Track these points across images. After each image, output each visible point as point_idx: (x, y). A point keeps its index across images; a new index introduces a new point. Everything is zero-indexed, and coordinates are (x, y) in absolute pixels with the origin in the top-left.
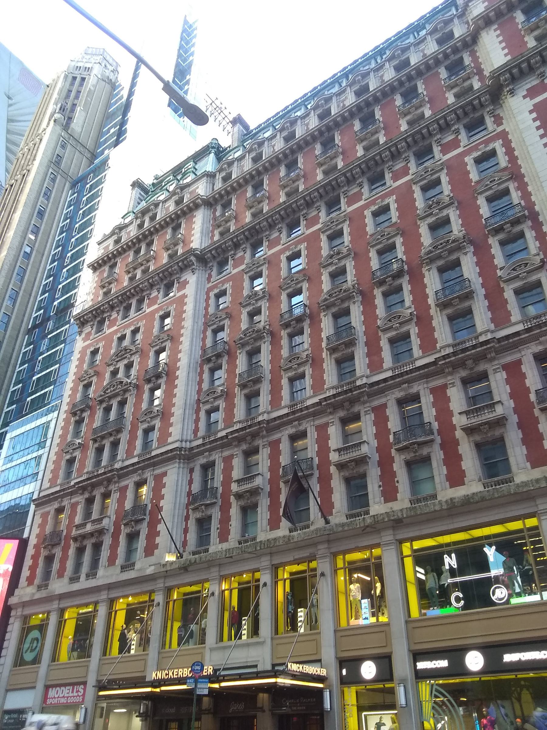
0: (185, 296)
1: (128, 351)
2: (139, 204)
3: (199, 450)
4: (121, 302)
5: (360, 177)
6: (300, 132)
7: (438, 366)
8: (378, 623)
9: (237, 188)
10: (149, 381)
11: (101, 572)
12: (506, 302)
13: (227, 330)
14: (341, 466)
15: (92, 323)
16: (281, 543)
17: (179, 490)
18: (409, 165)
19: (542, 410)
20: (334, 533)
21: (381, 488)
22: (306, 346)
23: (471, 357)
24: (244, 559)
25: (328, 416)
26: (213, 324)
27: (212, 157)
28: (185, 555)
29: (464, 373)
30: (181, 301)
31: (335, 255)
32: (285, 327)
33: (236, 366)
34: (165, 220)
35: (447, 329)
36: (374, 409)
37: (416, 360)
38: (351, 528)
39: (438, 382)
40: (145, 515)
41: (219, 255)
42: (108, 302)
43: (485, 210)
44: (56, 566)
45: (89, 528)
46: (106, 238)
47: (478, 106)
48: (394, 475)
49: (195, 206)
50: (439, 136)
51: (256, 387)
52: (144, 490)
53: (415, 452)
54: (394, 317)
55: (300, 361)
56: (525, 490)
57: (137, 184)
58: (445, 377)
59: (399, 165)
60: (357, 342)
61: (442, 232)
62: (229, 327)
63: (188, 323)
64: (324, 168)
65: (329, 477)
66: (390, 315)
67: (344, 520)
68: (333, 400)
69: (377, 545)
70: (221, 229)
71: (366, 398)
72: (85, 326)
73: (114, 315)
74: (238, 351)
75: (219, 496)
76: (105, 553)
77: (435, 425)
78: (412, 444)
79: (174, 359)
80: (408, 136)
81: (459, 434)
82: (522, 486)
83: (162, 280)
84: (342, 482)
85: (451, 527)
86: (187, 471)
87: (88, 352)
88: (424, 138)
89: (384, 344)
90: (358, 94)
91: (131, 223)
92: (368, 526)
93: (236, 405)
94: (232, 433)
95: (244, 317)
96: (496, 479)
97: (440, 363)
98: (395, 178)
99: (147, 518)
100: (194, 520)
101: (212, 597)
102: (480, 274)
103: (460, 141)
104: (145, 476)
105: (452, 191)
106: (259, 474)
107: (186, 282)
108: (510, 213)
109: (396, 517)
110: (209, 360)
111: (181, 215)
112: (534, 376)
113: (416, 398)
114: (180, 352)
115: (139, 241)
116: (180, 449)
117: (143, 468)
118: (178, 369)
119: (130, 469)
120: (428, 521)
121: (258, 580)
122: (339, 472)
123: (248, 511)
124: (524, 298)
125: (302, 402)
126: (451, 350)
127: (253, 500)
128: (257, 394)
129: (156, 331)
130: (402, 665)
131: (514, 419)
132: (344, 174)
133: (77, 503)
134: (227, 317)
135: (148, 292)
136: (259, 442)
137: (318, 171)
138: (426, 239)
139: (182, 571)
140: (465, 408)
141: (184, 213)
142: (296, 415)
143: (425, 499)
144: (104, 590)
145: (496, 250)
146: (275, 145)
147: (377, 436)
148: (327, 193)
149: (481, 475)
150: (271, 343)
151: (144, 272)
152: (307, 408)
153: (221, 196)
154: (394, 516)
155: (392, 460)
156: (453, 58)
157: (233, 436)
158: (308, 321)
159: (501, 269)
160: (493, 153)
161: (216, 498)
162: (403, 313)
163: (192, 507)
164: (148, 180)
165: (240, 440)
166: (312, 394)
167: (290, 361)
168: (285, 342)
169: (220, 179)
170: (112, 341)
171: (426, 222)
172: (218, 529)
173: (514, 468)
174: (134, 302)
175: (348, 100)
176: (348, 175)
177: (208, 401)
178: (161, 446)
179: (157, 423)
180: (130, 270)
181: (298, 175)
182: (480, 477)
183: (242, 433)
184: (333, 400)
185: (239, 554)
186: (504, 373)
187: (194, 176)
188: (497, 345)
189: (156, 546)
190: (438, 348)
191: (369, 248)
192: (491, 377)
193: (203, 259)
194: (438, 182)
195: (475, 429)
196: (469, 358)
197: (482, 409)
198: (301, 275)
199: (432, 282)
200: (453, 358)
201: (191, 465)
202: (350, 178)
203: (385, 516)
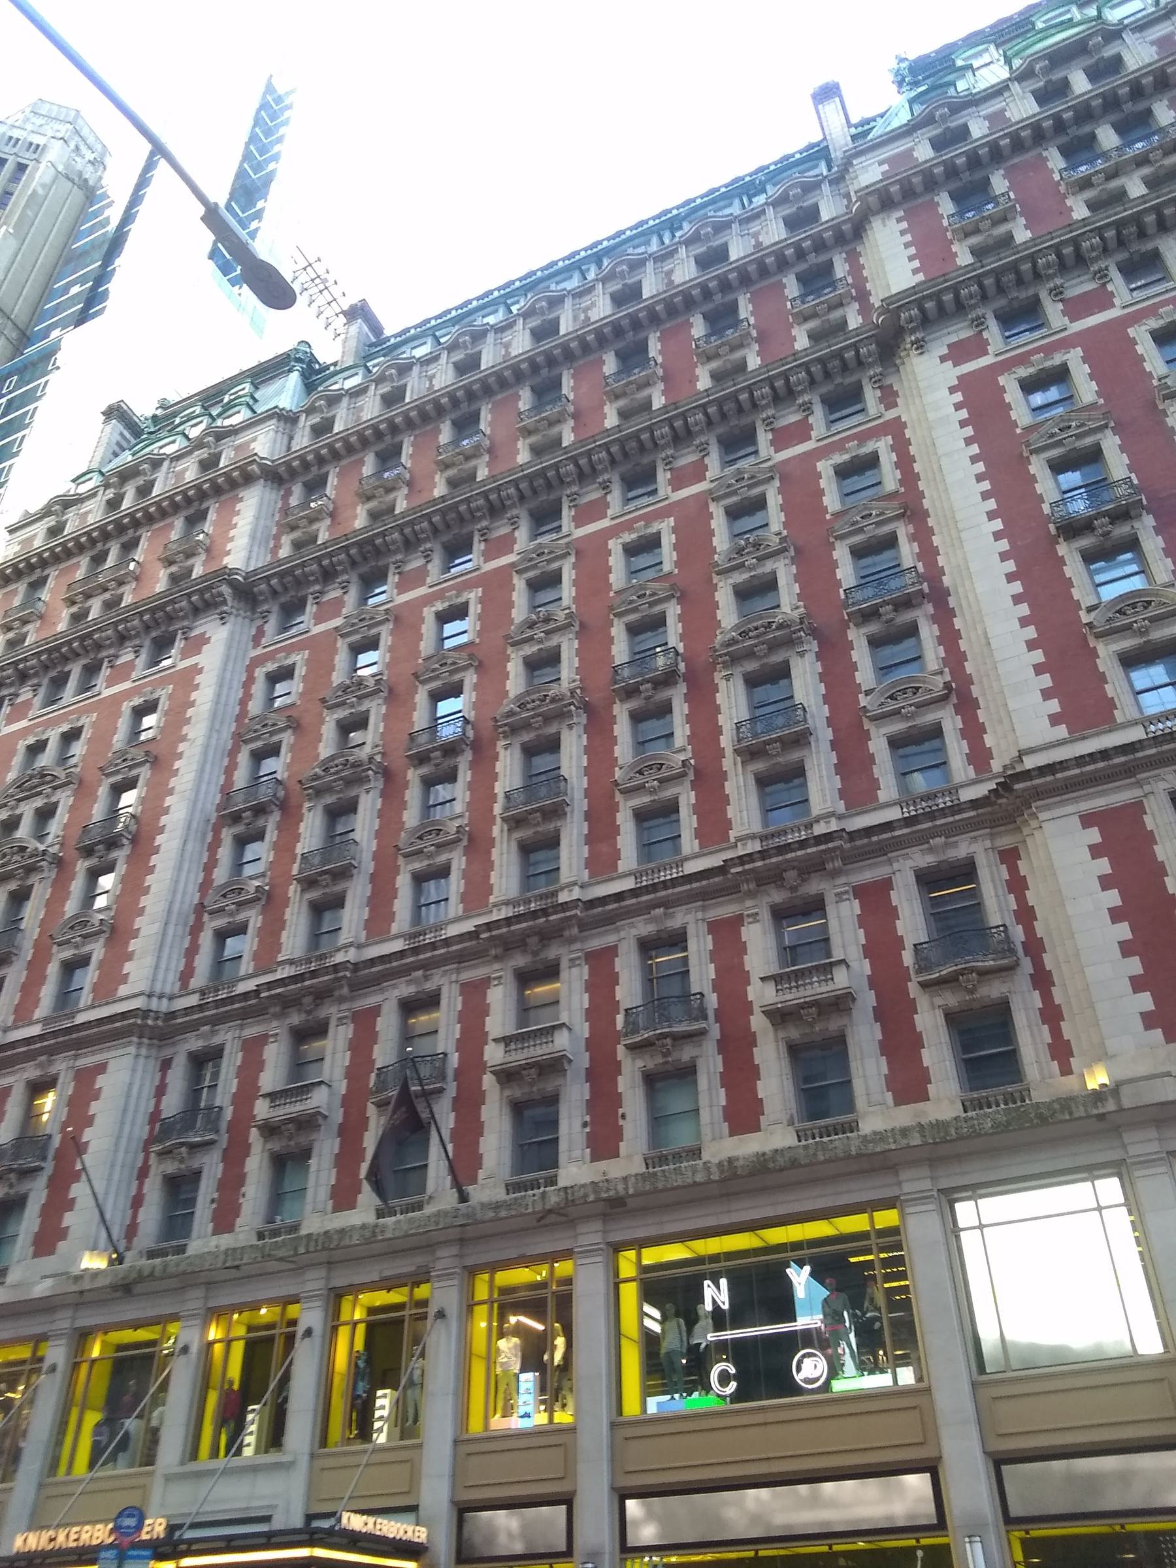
0: (196, 670)
1: (48, 778)
2: (116, 455)
3: (188, 1018)
4: (46, 668)
5: (605, 470)
6: (489, 358)
7: (730, 876)
8: (552, 1427)
9: (343, 452)
10: (88, 852)
12: (871, 759)
13: (285, 755)
14: (506, 1076)
17: (131, 1108)
18: (707, 460)
19: (924, 985)
21: (588, 1130)
22: (458, 807)
23: (795, 864)
24: (266, 1274)
25: (490, 963)
26: (255, 739)
27: (294, 380)
28: (129, 1257)
29: (778, 896)
30: (187, 680)
31: (540, 621)
32: (416, 762)
33: (297, 837)
34: (171, 498)
35: (754, 800)
36: (592, 957)
37: (686, 859)
38: (514, 1212)
39: (725, 910)
40: (44, 1159)
41: (286, 589)
42: (16, 663)
43: (846, 572)
46: (29, 521)
47: (852, 364)
48: (617, 1100)
49: (241, 478)
50: (771, 412)
51: (338, 888)
52: (48, 1102)
53: (665, 1055)
54: (650, 767)
55: (441, 839)
56: (878, 1149)
57: (116, 413)
58: (741, 900)
59: (687, 458)
60: (568, 809)
61: (760, 604)
62: (292, 748)
63: (197, 731)
64: (533, 439)
65: (478, 1098)
66: (643, 760)
67: (500, 1194)
68: (504, 930)
69: (567, 1254)
70: (296, 535)
71: (575, 930)
73: (25, 694)
74: (307, 805)
75: (224, 1126)
77: (712, 1001)
79: (154, 807)
80: (710, 402)
81: (758, 1022)
82: (873, 1141)
83: (148, 628)
84: (506, 1110)
85: (725, 1220)
86: (153, 1066)
88: (740, 410)
89: (625, 820)
90: (618, 300)
91: (92, 494)
92: (550, 1211)
93: (288, 924)
94: (270, 985)
95: (329, 730)
96: (822, 1122)
97: (733, 871)
98: (677, 483)
99: (49, 1166)
100: (159, 1179)
101: (183, 1358)
102: (826, 699)
104: (53, 1070)
105: (786, 525)
106: (322, 1082)
107: (203, 640)
108: (894, 584)
109: (612, 1193)
110: (236, 818)
111: (210, 492)
112: (913, 914)
113: (678, 940)
114: (171, 792)
115: (106, 536)
116: (145, 1013)
117: (52, 1052)
118: (161, 830)
119: (22, 1050)
121: (293, 1323)
122: (502, 1089)
123: (288, 1163)
124: (906, 756)
125: (438, 928)
126: (756, 846)
127: (303, 1140)
128: (338, 902)
129: (119, 739)
131: (868, 999)
132: (574, 460)
134: (289, 727)
135: (112, 651)
136: (331, 1011)
137: (520, 444)
138: (728, 614)
139: (119, 1294)
140: (774, 969)
141: (217, 490)
142: (422, 957)
143: (677, 1157)
145: (861, 654)
146: (434, 376)
147: (590, 1014)
148: (535, 492)
149: (794, 1111)
151: (109, 605)
152: (447, 942)
153: (306, 465)
154: (608, 1190)
155: (617, 1068)
157: (273, 992)
158: (468, 755)
159: (868, 693)
160: (872, 461)
161: (217, 1132)
162: (667, 760)
163: (157, 1148)
164: (144, 408)
165: (287, 1003)
166: (460, 913)
167: (420, 838)
168: (413, 795)
169: (308, 429)
170: (13, 752)
171: (731, 581)
172: (213, 1201)
173: (860, 1102)
174: (76, 670)
175: (595, 310)
176: (583, 462)
177: (222, 910)
178: (99, 1002)
179: (97, 950)
180: (77, 598)
181: (478, 447)
182: (792, 1115)
185: (255, 1261)
186: (856, 904)
187: (249, 414)
188: (848, 845)
189: (63, 1234)
190: (732, 840)
191: (612, 617)
192: (830, 909)
193: (248, 593)
194: (760, 504)
195: (791, 1014)
197: (807, 973)
198: (464, 655)
199: (732, 702)
200: (760, 864)
201: (167, 1052)
202: (587, 469)
203: (590, 1190)
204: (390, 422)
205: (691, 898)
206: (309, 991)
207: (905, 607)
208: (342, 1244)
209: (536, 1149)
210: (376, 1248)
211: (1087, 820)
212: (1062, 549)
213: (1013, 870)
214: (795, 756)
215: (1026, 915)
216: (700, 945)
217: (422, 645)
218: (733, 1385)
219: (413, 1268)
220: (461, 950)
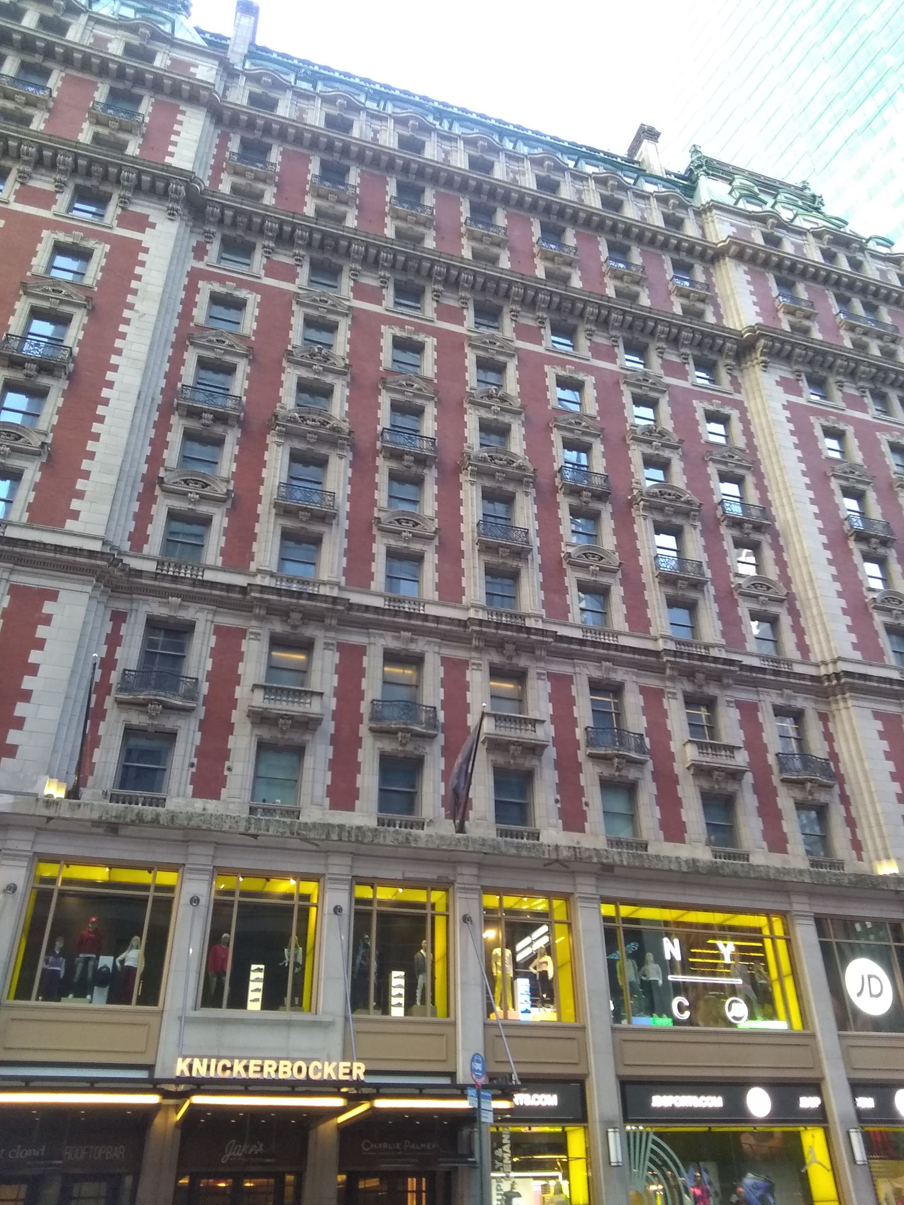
3: (157, 583)
16: (389, 841)
20: (502, 854)
24: (285, 849)
48: (580, 791)
54: (594, 555)
60: (529, 557)
66: (589, 548)
78: (618, 756)
81: (679, 768)
84: (491, 771)
92: (557, 861)
94: (263, 589)
103: (296, 275)
107: (142, 223)
109: (610, 861)
120: (649, 881)
130: (603, 1098)
134: (246, 356)
136: (319, 636)
142: (413, 622)
150: (352, 465)
152: (426, 617)
155: (579, 768)
156: (683, 256)
157: (266, 596)
165: (272, 611)
184: (494, 631)
193: (193, 204)
196: (700, 670)
204: (603, 220)
205: (630, 664)
207: (755, 530)
208: (376, 841)
209: (513, 806)
210: (402, 852)
211: (877, 715)
212: (852, 544)
213: (826, 726)
214: (693, 595)
215: (834, 756)
216: (433, 671)
217: (382, 356)
218: (687, 1015)
219: (435, 877)
220: (446, 630)
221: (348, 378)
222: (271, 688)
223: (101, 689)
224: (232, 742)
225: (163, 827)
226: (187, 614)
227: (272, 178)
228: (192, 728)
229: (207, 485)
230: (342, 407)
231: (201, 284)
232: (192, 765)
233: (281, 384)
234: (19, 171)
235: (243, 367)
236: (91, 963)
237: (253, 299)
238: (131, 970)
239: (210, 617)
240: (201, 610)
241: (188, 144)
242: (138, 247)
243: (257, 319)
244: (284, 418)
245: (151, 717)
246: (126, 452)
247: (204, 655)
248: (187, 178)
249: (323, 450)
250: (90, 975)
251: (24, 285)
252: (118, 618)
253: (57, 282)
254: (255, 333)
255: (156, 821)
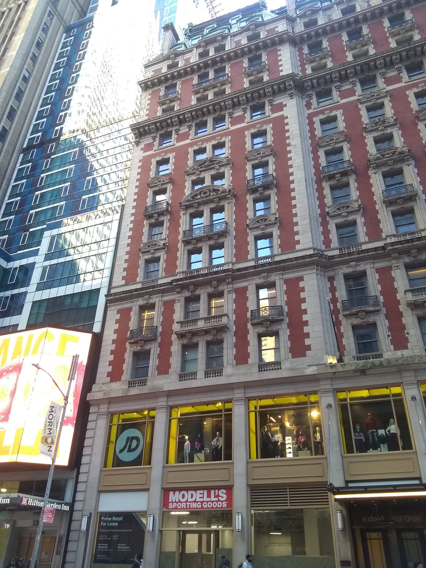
0: (283, 118)
3: (342, 259)
10: (254, 191)
11: (228, 370)
15: (154, 135)
28: (346, 359)
44: (153, 362)
45: (201, 324)
72: (143, 137)
76: (229, 351)
87: (154, 161)
94: (392, 244)
107: (281, 107)
119: (251, 271)
133: (172, 302)
139: (358, 374)
144: (239, 388)
157: (395, 247)
165: (401, 253)
170: (188, 153)
183: (407, 245)
189: (309, 348)
201: (331, 274)
206: (414, 247)
221: (398, 125)
222: (414, 290)
223: (335, 312)
224: (404, 321)
225: (386, 367)
226: (362, 267)
227: (328, 54)
228: (382, 318)
229: (348, 207)
230: (400, 141)
231: (314, 119)
232: (389, 336)
233: (366, 145)
234: (228, 113)
235: (346, 146)
236: (375, 434)
237: (339, 113)
238: (394, 435)
239: (372, 266)
240: (366, 264)
241: (287, 62)
242: (283, 118)
243: (344, 121)
244: (373, 160)
245: (362, 319)
246: (309, 208)
247: (375, 284)
248: (291, 76)
249: (398, 166)
250: (376, 439)
251: (246, 158)
252: (331, 279)
253: (258, 150)
254: (346, 128)
255: (381, 365)
